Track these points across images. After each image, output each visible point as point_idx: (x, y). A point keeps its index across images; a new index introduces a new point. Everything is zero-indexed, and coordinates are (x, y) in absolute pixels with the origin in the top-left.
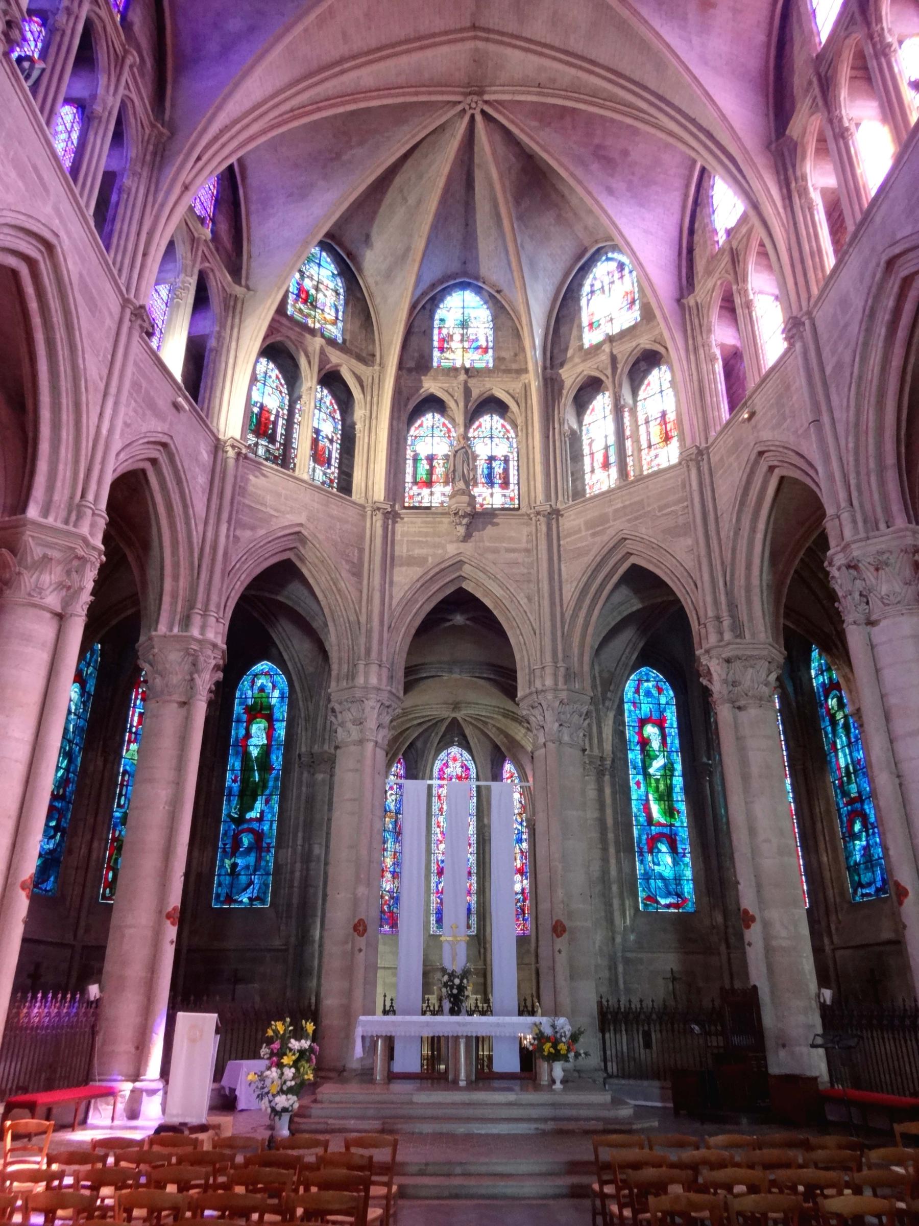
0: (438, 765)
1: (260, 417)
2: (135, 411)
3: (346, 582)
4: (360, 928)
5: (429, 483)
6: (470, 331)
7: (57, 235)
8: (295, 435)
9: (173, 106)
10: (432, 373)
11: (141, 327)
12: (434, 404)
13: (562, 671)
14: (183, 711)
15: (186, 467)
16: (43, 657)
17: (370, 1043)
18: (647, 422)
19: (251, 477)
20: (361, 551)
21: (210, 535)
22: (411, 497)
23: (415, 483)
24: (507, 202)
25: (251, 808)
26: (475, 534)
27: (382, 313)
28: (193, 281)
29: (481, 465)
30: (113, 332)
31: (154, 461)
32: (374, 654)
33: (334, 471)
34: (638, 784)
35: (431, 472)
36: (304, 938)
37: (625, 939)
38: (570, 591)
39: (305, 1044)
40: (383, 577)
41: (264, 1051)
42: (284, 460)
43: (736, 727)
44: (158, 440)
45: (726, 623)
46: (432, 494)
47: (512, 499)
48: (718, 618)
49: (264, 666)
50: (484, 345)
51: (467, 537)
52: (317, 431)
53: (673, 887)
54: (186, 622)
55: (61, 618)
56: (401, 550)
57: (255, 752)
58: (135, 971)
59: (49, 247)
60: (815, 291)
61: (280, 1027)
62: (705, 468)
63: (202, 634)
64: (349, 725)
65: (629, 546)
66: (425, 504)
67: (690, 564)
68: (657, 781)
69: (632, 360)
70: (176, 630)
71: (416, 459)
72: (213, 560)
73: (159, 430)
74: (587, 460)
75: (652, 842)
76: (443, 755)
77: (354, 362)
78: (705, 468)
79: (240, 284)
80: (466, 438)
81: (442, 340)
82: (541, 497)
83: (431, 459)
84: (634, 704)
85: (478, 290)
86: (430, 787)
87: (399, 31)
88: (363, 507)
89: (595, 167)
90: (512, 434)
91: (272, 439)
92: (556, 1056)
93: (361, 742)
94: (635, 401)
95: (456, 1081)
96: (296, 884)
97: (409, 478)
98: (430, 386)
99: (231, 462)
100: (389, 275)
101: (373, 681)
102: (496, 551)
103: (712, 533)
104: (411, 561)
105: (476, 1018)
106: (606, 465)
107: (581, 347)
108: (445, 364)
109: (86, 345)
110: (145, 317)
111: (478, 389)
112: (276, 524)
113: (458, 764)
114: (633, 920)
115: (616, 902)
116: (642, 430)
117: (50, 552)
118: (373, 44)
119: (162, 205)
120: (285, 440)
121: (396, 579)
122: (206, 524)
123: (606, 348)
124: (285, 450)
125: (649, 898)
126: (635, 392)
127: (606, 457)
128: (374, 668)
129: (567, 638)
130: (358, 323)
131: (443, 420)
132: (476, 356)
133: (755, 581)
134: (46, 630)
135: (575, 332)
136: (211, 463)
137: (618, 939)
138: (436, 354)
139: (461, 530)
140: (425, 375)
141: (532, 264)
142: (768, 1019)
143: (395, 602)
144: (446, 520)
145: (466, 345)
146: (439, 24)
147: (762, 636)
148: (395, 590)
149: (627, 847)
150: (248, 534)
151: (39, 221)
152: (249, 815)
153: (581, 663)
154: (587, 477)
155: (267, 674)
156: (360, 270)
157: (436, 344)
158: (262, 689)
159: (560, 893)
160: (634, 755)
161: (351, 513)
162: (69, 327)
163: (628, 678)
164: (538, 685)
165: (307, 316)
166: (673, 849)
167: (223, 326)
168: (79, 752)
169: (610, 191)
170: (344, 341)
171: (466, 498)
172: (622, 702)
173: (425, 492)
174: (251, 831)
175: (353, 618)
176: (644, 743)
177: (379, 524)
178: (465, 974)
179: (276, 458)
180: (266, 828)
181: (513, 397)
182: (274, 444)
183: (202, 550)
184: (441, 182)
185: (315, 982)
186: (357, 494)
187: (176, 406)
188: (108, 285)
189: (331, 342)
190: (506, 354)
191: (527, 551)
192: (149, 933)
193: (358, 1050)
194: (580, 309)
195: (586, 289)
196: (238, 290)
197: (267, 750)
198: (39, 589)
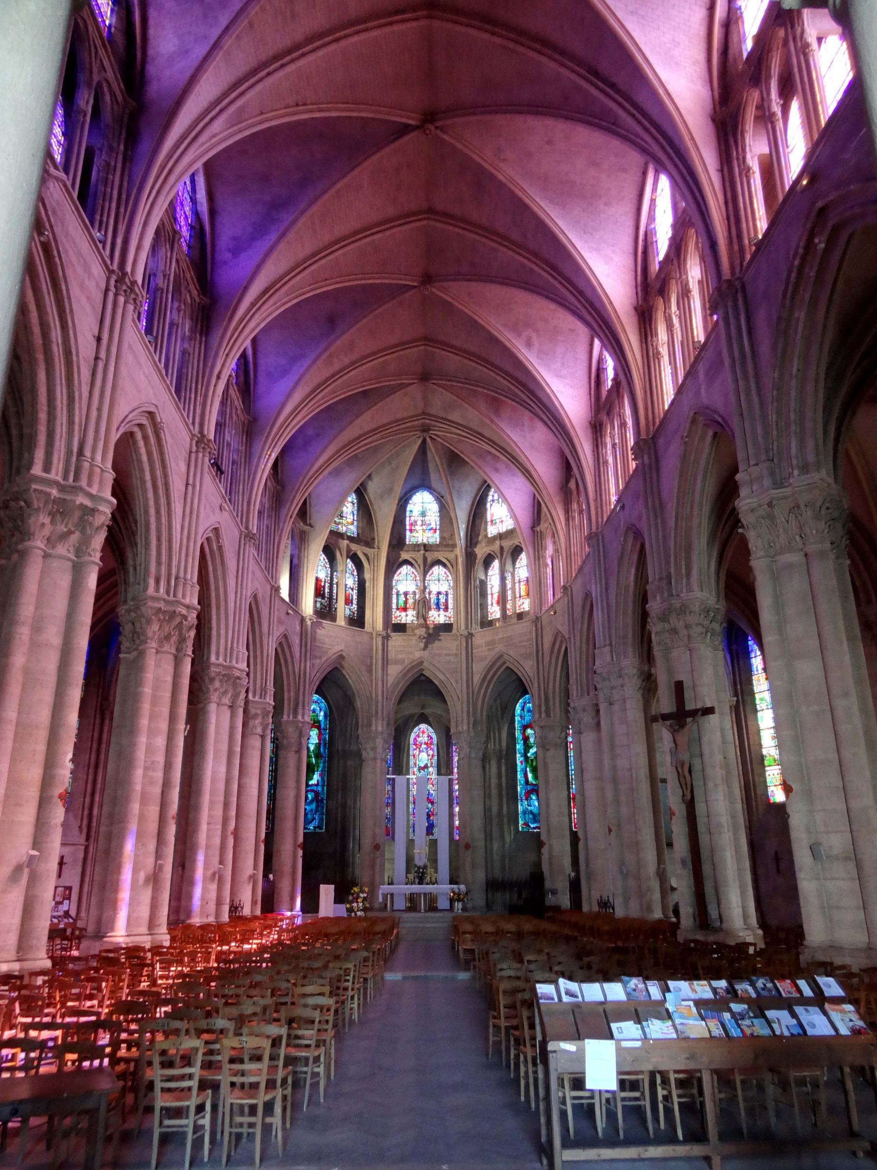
0: (413, 736)
3: (365, 678)
4: (377, 847)
5: (405, 609)
6: (427, 518)
8: (335, 591)
9: (282, 472)
10: (405, 548)
12: (406, 562)
13: (472, 722)
14: (297, 755)
16: (258, 753)
17: (385, 896)
18: (520, 582)
19: (318, 630)
20: (371, 658)
21: (302, 668)
22: (396, 618)
23: (398, 609)
24: (444, 470)
25: (312, 779)
26: (430, 646)
27: (378, 515)
28: (289, 541)
29: (433, 597)
32: (380, 714)
33: (355, 607)
34: (521, 762)
35: (406, 602)
36: (344, 848)
37: (510, 845)
38: (477, 679)
39: (365, 895)
40: (383, 670)
41: (351, 898)
43: (545, 758)
45: (543, 708)
46: (407, 615)
47: (450, 618)
48: (540, 706)
49: (316, 697)
50: (433, 526)
51: (424, 649)
52: (346, 585)
53: (535, 818)
54: (295, 714)
55: (263, 737)
56: (392, 655)
57: (312, 747)
58: (287, 869)
60: (574, 575)
61: (356, 889)
62: (539, 626)
63: (303, 718)
64: (369, 750)
65: (506, 657)
66: (403, 622)
67: (531, 675)
68: (532, 760)
69: (510, 551)
70: (291, 717)
71: (398, 594)
72: (305, 680)
74: (489, 597)
75: (528, 795)
76: (416, 729)
77: (364, 547)
78: (539, 626)
79: (307, 525)
80: (425, 588)
81: (411, 525)
82: (463, 627)
83: (406, 594)
84: (521, 717)
85: (431, 493)
86: (408, 779)
87: (386, 420)
88: (371, 634)
89: (488, 458)
90: (450, 578)
91: (323, 597)
92: (459, 900)
93: (375, 759)
94: (514, 568)
95: (420, 911)
96: (339, 819)
97: (394, 606)
98: (404, 556)
99: (309, 627)
100: (382, 497)
101: (380, 729)
102: (440, 655)
103: (540, 662)
104: (397, 662)
105: (431, 886)
106: (498, 603)
107: (486, 536)
108: (414, 541)
111: (431, 556)
112: (330, 653)
113: (425, 735)
114: (515, 837)
115: (506, 827)
116: (517, 585)
118: (374, 426)
119: (282, 529)
121: (389, 672)
122: (300, 661)
123: (498, 542)
125: (524, 824)
126: (514, 563)
127: (498, 597)
128: (380, 722)
129: (475, 705)
130: (365, 521)
131: (412, 570)
132: (429, 534)
133: (557, 689)
134: (256, 742)
135: (483, 526)
137: (507, 845)
138: (408, 533)
139: (422, 645)
140: (402, 550)
141: (459, 492)
142: (548, 885)
143: (389, 685)
144: (413, 638)
145: (424, 527)
146: (406, 414)
147: (558, 716)
148: (389, 678)
149: (513, 798)
150: (318, 661)
152: (311, 783)
153: (482, 715)
154: (489, 607)
155: (316, 702)
156: (366, 490)
157: (408, 527)
158: (314, 711)
159: (468, 831)
160: (519, 746)
161: (366, 638)
162: (259, 617)
163: (517, 702)
164: (460, 728)
165: (338, 524)
166: (538, 799)
167: (300, 551)
169: (497, 470)
170: (358, 534)
171: (424, 630)
172: (514, 716)
173: (403, 614)
174: (312, 791)
175: (368, 695)
176: (526, 739)
177: (380, 643)
178: (425, 867)
180: (320, 788)
181: (449, 562)
183: (299, 674)
184: (409, 463)
185: (351, 869)
186: (368, 627)
187: (288, 614)
189: (351, 539)
190: (446, 535)
191: (456, 655)
192: (292, 854)
193: (381, 899)
194: (486, 509)
195: (490, 498)
196: (306, 528)
197: (318, 746)
198: (255, 727)
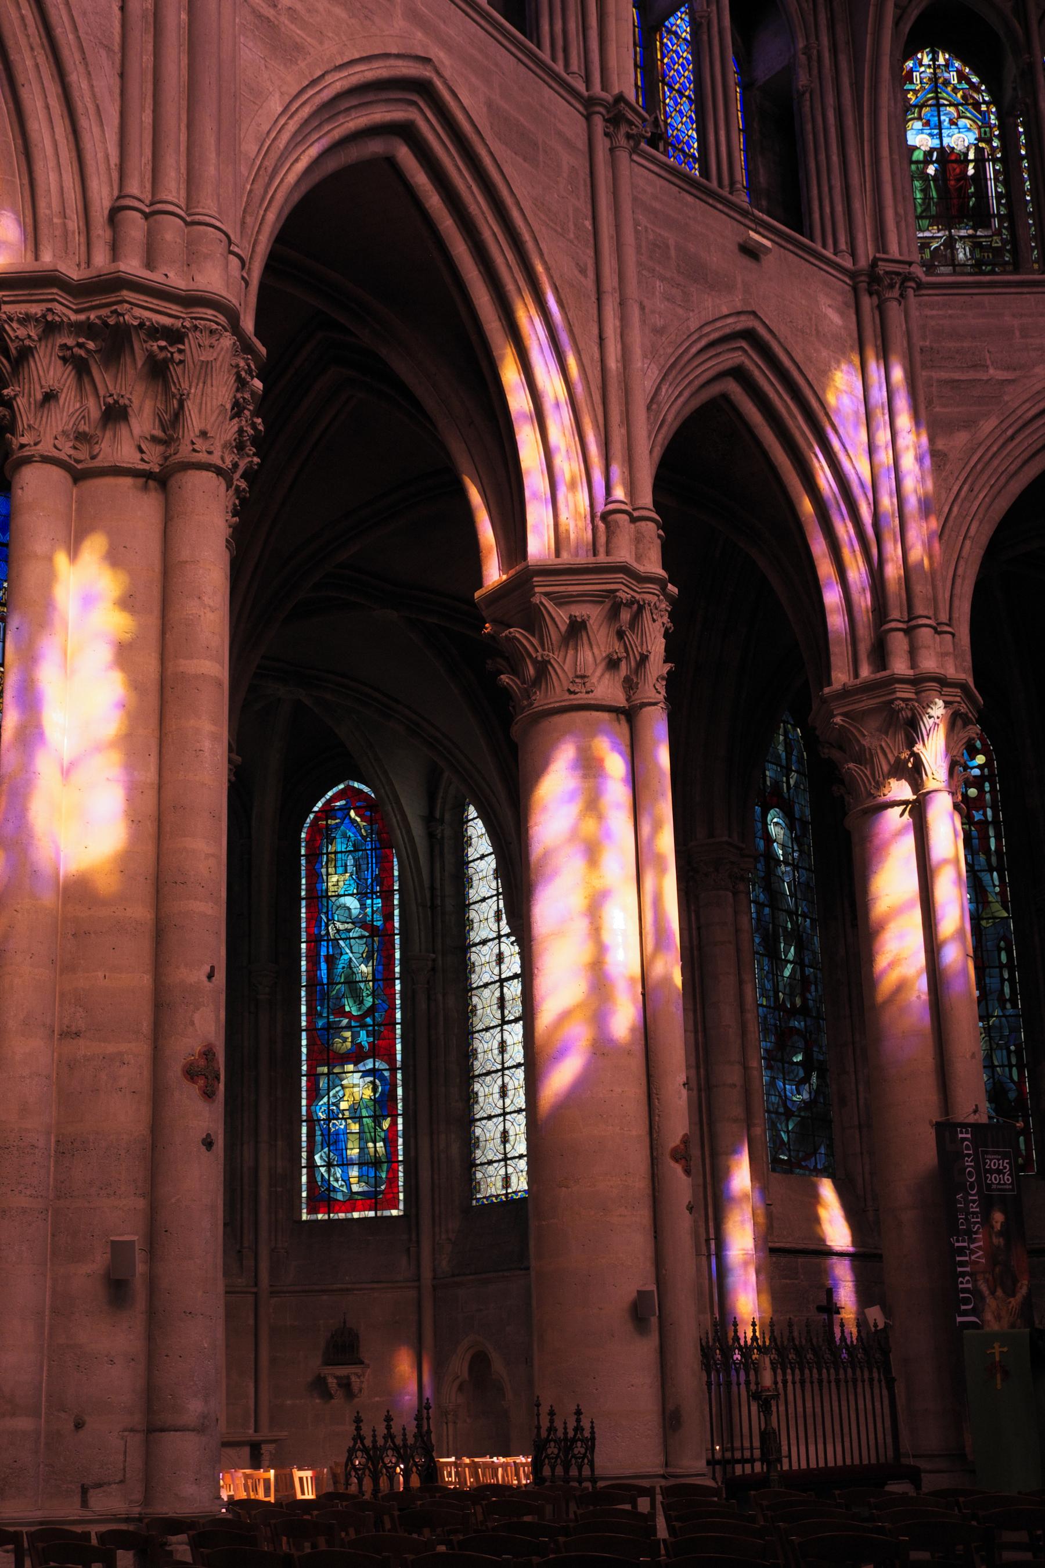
1: (945, 180)
2: (670, 299)
7: (426, 60)
11: (629, 137)
15: (799, 358)
30: (584, 173)
31: (738, 373)
42: (1015, 252)
44: (727, 331)
59: (423, 88)
73: (725, 311)
109: (536, 227)
110: (630, 115)
117: (579, 611)
120: (1009, 206)
124: (1012, 229)
136: (853, 326)
151: (387, 56)
168: (813, 927)
179: (998, 252)
182: (987, 226)
187: (750, 252)
188: (547, 92)
